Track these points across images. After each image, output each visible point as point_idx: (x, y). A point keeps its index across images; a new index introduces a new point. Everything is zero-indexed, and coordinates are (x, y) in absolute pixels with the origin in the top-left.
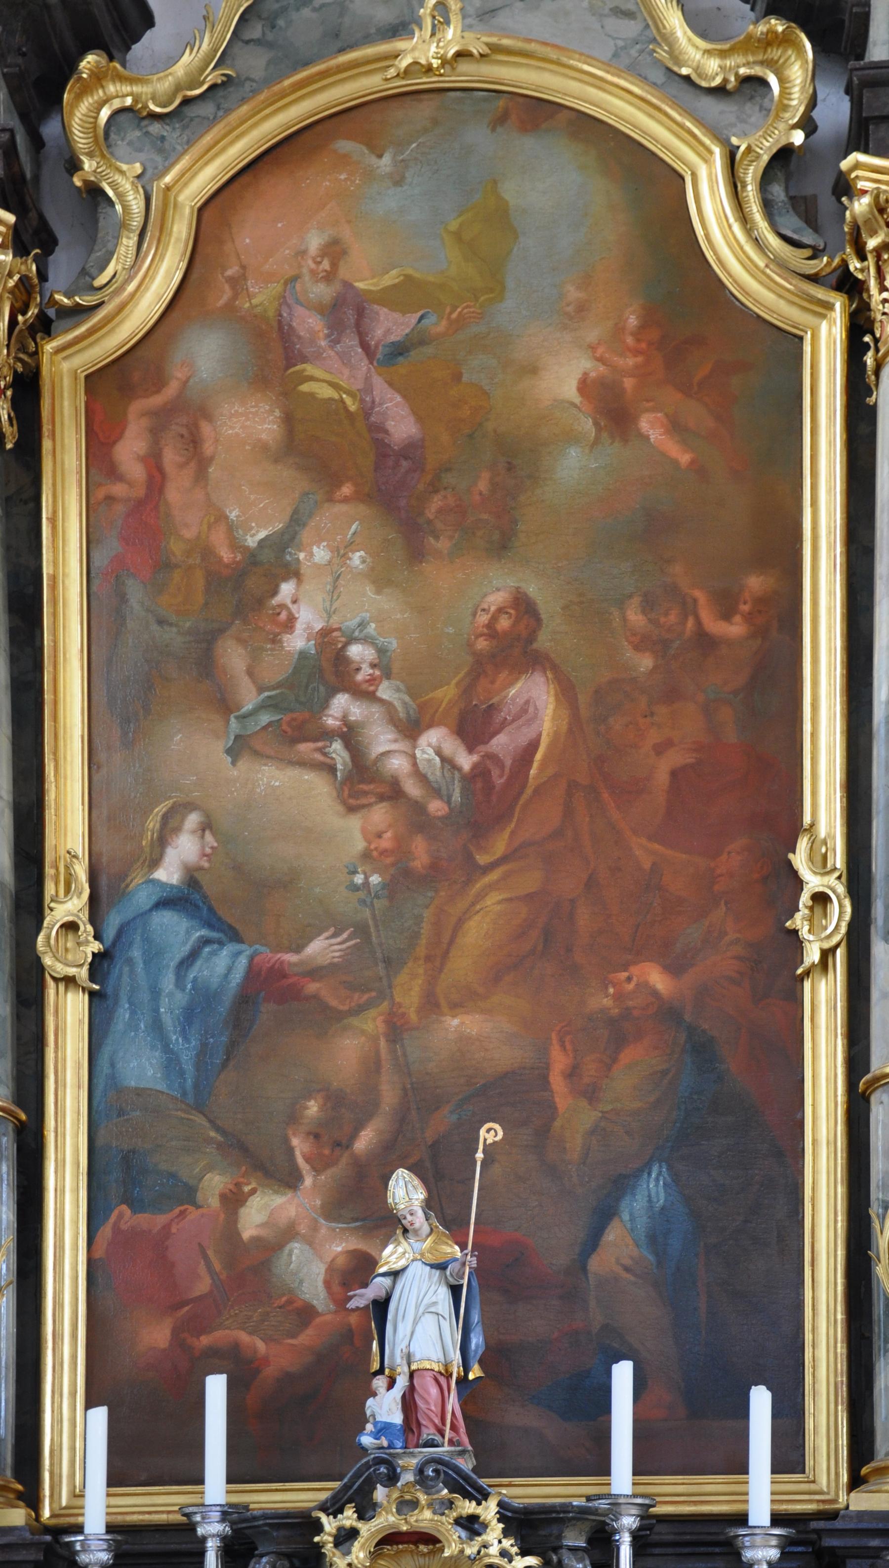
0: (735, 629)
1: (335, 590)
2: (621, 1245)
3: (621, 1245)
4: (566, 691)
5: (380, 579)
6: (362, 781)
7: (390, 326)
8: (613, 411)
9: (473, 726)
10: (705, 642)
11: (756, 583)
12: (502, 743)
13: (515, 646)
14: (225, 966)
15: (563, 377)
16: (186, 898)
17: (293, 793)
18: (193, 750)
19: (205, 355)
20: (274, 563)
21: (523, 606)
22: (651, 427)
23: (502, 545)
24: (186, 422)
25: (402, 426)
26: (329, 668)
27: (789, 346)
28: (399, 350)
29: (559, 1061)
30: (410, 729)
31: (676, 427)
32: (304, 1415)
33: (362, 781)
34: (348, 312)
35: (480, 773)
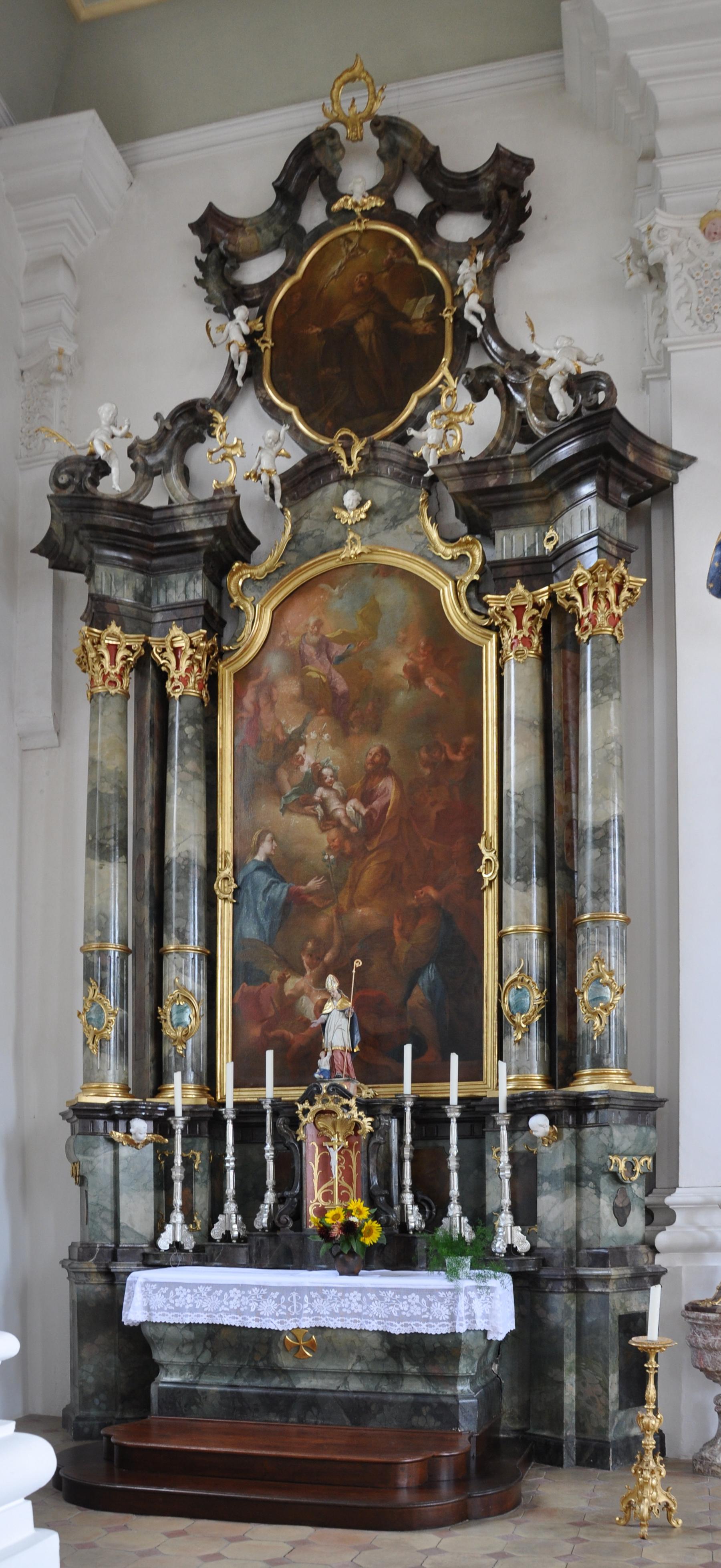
0: (459, 757)
1: (319, 750)
2: (419, 995)
3: (419, 995)
4: (399, 783)
5: (334, 743)
6: (328, 821)
7: (338, 650)
8: (415, 676)
9: (366, 798)
10: (449, 763)
11: (467, 740)
12: (376, 804)
13: (381, 767)
14: (280, 892)
15: (398, 666)
16: (266, 866)
17: (303, 825)
18: (269, 811)
19: (274, 663)
20: (297, 739)
21: (383, 752)
22: (429, 683)
23: (376, 730)
24: (268, 687)
25: (342, 686)
26: (316, 778)
27: (477, 652)
28: (341, 658)
29: (397, 924)
30: (344, 800)
31: (438, 682)
32: (299, 1064)
33: (328, 821)
34: (323, 646)
35: (369, 816)
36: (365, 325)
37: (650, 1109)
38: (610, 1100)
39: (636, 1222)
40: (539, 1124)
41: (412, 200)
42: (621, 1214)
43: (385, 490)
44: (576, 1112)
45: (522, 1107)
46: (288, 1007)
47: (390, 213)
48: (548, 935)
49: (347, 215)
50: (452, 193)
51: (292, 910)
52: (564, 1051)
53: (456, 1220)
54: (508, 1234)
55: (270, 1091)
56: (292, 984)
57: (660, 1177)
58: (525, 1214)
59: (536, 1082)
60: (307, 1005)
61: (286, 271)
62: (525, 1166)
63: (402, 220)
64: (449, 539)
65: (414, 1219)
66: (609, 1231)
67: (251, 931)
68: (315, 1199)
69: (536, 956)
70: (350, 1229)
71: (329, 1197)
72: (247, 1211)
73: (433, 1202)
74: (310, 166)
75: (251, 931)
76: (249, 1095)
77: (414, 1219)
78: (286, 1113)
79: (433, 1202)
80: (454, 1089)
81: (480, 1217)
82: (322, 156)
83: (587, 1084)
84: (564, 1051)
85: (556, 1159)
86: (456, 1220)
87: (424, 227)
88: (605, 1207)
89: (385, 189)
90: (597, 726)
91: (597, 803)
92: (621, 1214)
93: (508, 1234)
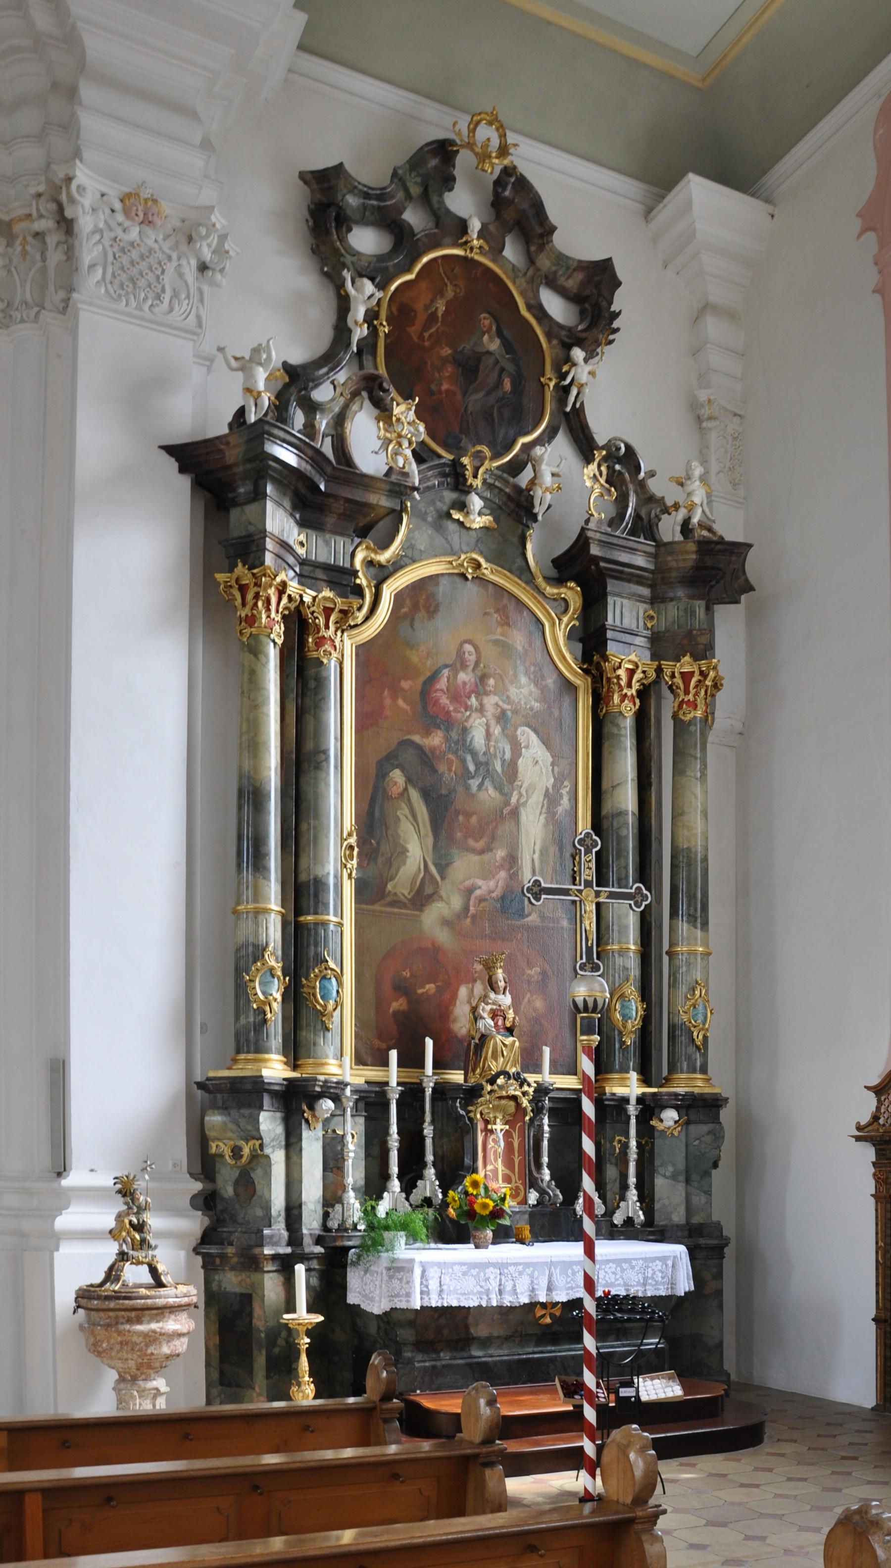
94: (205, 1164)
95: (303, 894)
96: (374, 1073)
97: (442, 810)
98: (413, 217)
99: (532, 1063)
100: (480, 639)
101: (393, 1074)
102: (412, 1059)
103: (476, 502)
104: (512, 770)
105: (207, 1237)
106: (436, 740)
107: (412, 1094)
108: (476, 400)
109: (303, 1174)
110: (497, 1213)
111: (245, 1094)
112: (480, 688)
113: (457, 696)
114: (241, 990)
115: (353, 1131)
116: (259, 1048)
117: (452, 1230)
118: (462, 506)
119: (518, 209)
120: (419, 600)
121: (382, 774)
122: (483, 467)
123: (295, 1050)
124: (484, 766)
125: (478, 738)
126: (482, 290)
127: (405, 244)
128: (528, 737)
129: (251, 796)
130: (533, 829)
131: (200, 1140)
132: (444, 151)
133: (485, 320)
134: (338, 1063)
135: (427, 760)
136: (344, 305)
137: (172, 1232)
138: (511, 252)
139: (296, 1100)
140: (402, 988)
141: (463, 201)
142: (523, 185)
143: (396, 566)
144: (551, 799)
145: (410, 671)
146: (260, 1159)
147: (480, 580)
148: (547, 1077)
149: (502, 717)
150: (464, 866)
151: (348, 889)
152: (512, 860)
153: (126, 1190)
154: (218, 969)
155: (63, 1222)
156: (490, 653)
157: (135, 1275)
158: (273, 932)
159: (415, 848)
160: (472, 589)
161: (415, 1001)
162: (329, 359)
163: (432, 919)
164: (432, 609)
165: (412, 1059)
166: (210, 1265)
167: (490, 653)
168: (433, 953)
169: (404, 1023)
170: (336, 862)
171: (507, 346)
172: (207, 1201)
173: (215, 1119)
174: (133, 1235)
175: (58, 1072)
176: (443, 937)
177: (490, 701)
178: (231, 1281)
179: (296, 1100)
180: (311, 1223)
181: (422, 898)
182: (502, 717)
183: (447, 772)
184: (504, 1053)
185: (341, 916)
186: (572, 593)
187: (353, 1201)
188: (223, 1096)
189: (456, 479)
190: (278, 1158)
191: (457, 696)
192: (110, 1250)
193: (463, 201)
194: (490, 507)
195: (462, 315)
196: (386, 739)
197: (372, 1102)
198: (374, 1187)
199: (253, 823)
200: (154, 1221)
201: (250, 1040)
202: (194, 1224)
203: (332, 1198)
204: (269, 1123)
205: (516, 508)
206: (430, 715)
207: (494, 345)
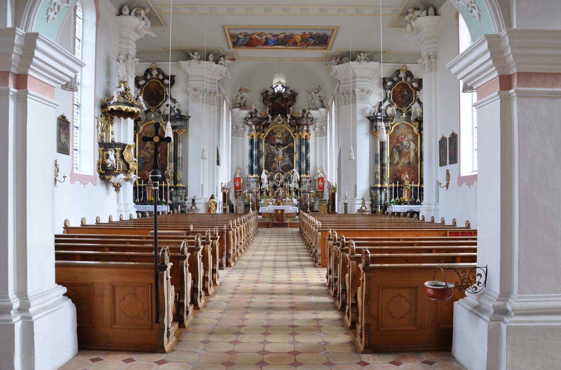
6: (149, 153)
14: (144, 161)
17: (146, 153)
18: (142, 151)
26: (148, 148)
33: (149, 153)
34: (149, 132)
36: (155, 93)
37: (185, 188)
38: (180, 187)
39: (183, 200)
40: (172, 189)
41: (161, 77)
42: (181, 199)
43: (157, 114)
44: (176, 188)
45: (171, 188)
46: (145, 174)
47: (158, 79)
48: (174, 168)
49: (153, 78)
50: (166, 77)
51: (145, 163)
52: (176, 182)
53: (164, 200)
54: (169, 201)
55: (143, 185)
56: (145, 172)
57: (186, 195)
58: (171, 199)
59: (173, 185)
60: (147, 175)
61: (145, 84)
62: (171, 194)
63: (159, 80)
64: (164, 121)
65: (159, 200)
66: (180, 201)
67: (140, 165)
68: (148, 197)
69: (173, 171)
70: (152, 201)
71: (149, 197)
72: (140, 199)
73: (161, 197)
74: (148, 71)
75: (140, 165)
76: (140, 185)
77: (159, 200)
78: (144, 187)
79: (161, 197)
80: (164, 185)
81: (166, 199)
82: (150, 70)
83: (178, 185)
84: (176, 182)
85: (174, 193)
86: (164, 200)
87: (162, 81)
88: (179, 199)
89: (157, 75)
90: (180, 147)
91: (180, 155)
92: (181, 199)
93: (169, 201)
94: (371, 196)
95: (383, 165)
96: (391, 185)
97: (400, 153)
98: (395, 79)
99: (411, 183)
100: (405, 131)
101: (393, 185)
102: (396, 183)
103: (404, 114)
104: (409, 147)
105: (371, 204)
106: (399, 144)
107: (395, 188)
108: (404, 100)
109: (382, 197)
110: (404, 201)
111: (375, 188)
112: (405, 137)
113: (402, 139)
114: (375, 177)
115: (388, 192)
116: (378, 183)
117: (399, 203)
118: (402, 115)
119: (409, 74)
120: (397, 128)
121: (392, 150)
122: (405, 109)
123: (382, 183)
124: (406, 147)
125: (405, 144)
126: (405, 86)
127: (394, 83)
128: (411, 142)
129: (376, 155)
130: (412, 154)
131: (371, 193)
132: (398, 71)
133: (405, 90)
134: (386, 185)
135: (398, 147)
136: (387, 94)
137: (368, 203)
138: (409, 79)
139: (381, 189)
140: (395, 175)
141: (402, 75)
142: (409, 71)
143: (394, 124)
144: (415, 150)
145: (396, 137)
146: (377, 195)
147: (405, 124)
148: (413, 185)
149: (408, 141)
150: (403, 160)
151: (388, 164)
152: (409, 158)
153: (363, 199)
154: (373, 174)
155: (356, 202)
156: (406, 133)
157: (364, 208)
158: (379, 170)
159: (397, 158)
160: (404, 125)
161: (397, 177)
162: (385, 101)
163: (399, 166)
164: (398, 129)
165: (396, 183)
166: (372, 207)
167: (406, 133)
168: (399, 170)
169: (396, 178)
170: (387, 161)
171: (408, 92)
172: (372, 200)
173: (372, 191)
174: (363, 204)
175: (356, 186)
176: (400, 168)
177: (406, 139)
178: (374, 209)
179: (381, 189)
180: (383, 203)
181: (398, 164)
182: (408, 141)
183: (401, 148)
184: (407, 183)
185: (388, 168)
186: (417, 124)
187: (388, 200)
188: (373, 189)
189: (401, 112)
190: (379, 195)
191: (402, 139)
192: (361, 205)
193: (402, 75)
194: (406, 114)
195: (402, 90)
196: (393, 145)
197: (391, 189)
198: (391, 199)
199: (377, 158)
200: (366, 202)
201: (376, 182)
202: (370, 203)
203: (386, 200)
204: (378, 192)
205: (409, 114)
206: (399, 141)
207: (406, 93)
